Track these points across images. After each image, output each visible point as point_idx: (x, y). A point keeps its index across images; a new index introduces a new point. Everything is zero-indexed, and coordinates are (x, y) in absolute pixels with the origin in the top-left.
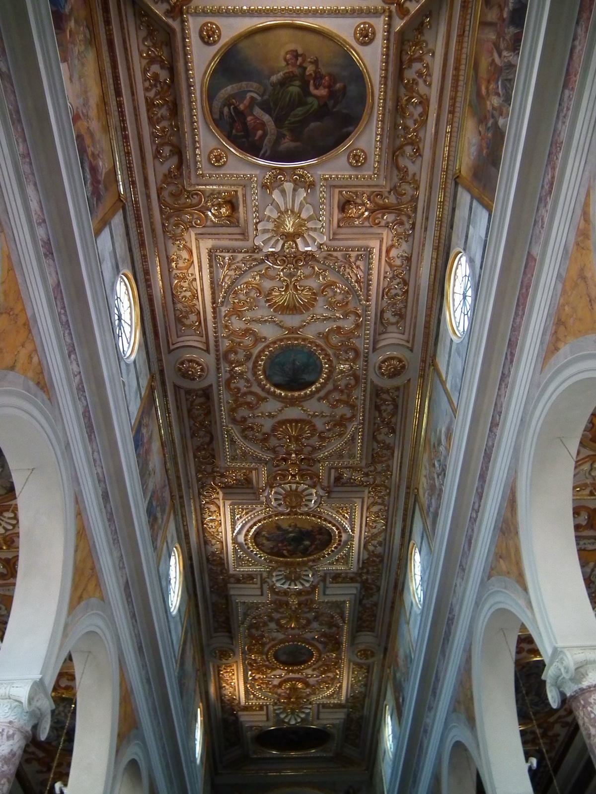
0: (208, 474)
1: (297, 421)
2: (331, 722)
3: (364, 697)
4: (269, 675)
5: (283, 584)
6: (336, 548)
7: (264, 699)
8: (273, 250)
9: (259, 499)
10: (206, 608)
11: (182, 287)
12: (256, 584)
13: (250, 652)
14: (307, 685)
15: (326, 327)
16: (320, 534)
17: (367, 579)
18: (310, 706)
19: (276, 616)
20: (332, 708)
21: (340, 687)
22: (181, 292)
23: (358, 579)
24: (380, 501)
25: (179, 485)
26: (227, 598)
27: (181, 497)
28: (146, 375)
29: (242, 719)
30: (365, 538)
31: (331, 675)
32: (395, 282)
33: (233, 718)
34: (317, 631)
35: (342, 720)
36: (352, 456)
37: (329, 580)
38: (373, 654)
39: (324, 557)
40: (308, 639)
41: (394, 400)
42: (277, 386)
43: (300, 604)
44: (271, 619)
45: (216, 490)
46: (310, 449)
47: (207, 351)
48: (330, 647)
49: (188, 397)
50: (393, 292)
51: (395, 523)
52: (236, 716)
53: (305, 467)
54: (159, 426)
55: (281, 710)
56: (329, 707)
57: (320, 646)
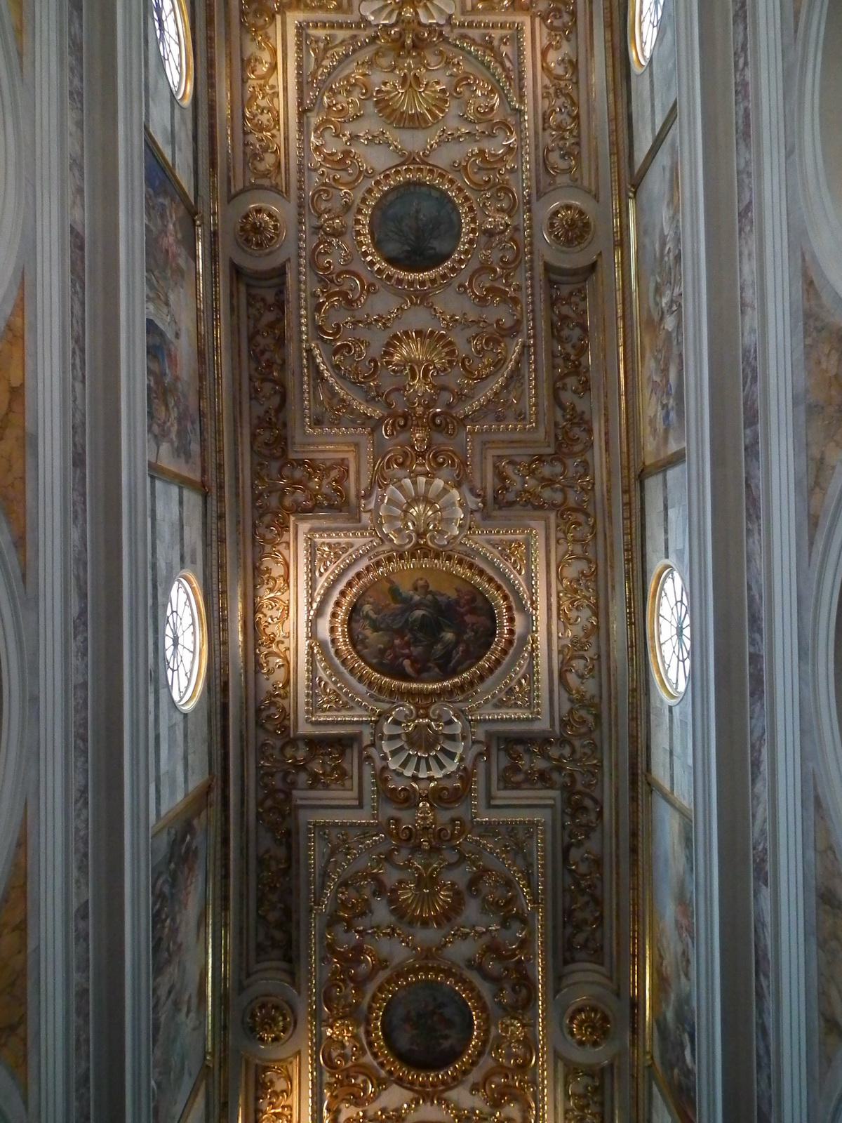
8: (387, 22)
9: (360, 521)
16: (473, 611)
30: (560, 652)
51: (613, 587)
54: (197, 273)
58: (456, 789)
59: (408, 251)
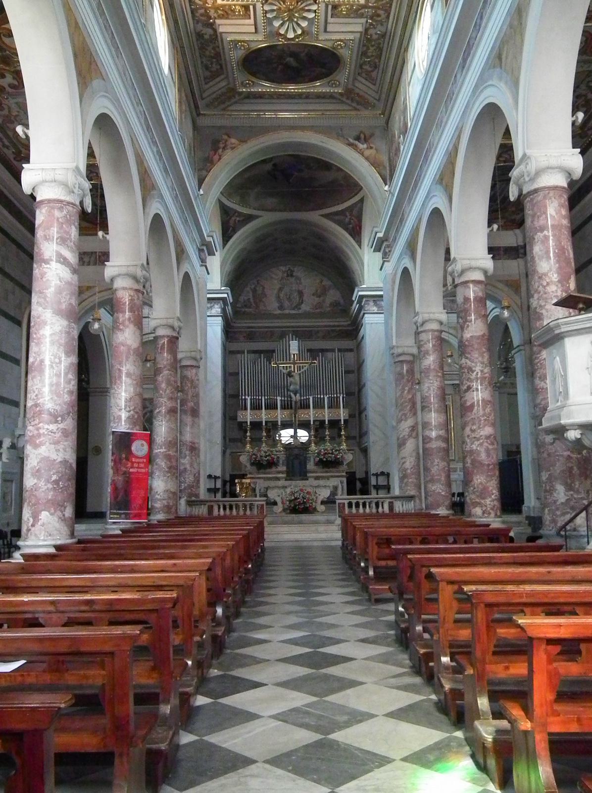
18: (314, 7)
29: (221, 29)
35: (358, 35)
52: (212, 26)
55: (274, 14)
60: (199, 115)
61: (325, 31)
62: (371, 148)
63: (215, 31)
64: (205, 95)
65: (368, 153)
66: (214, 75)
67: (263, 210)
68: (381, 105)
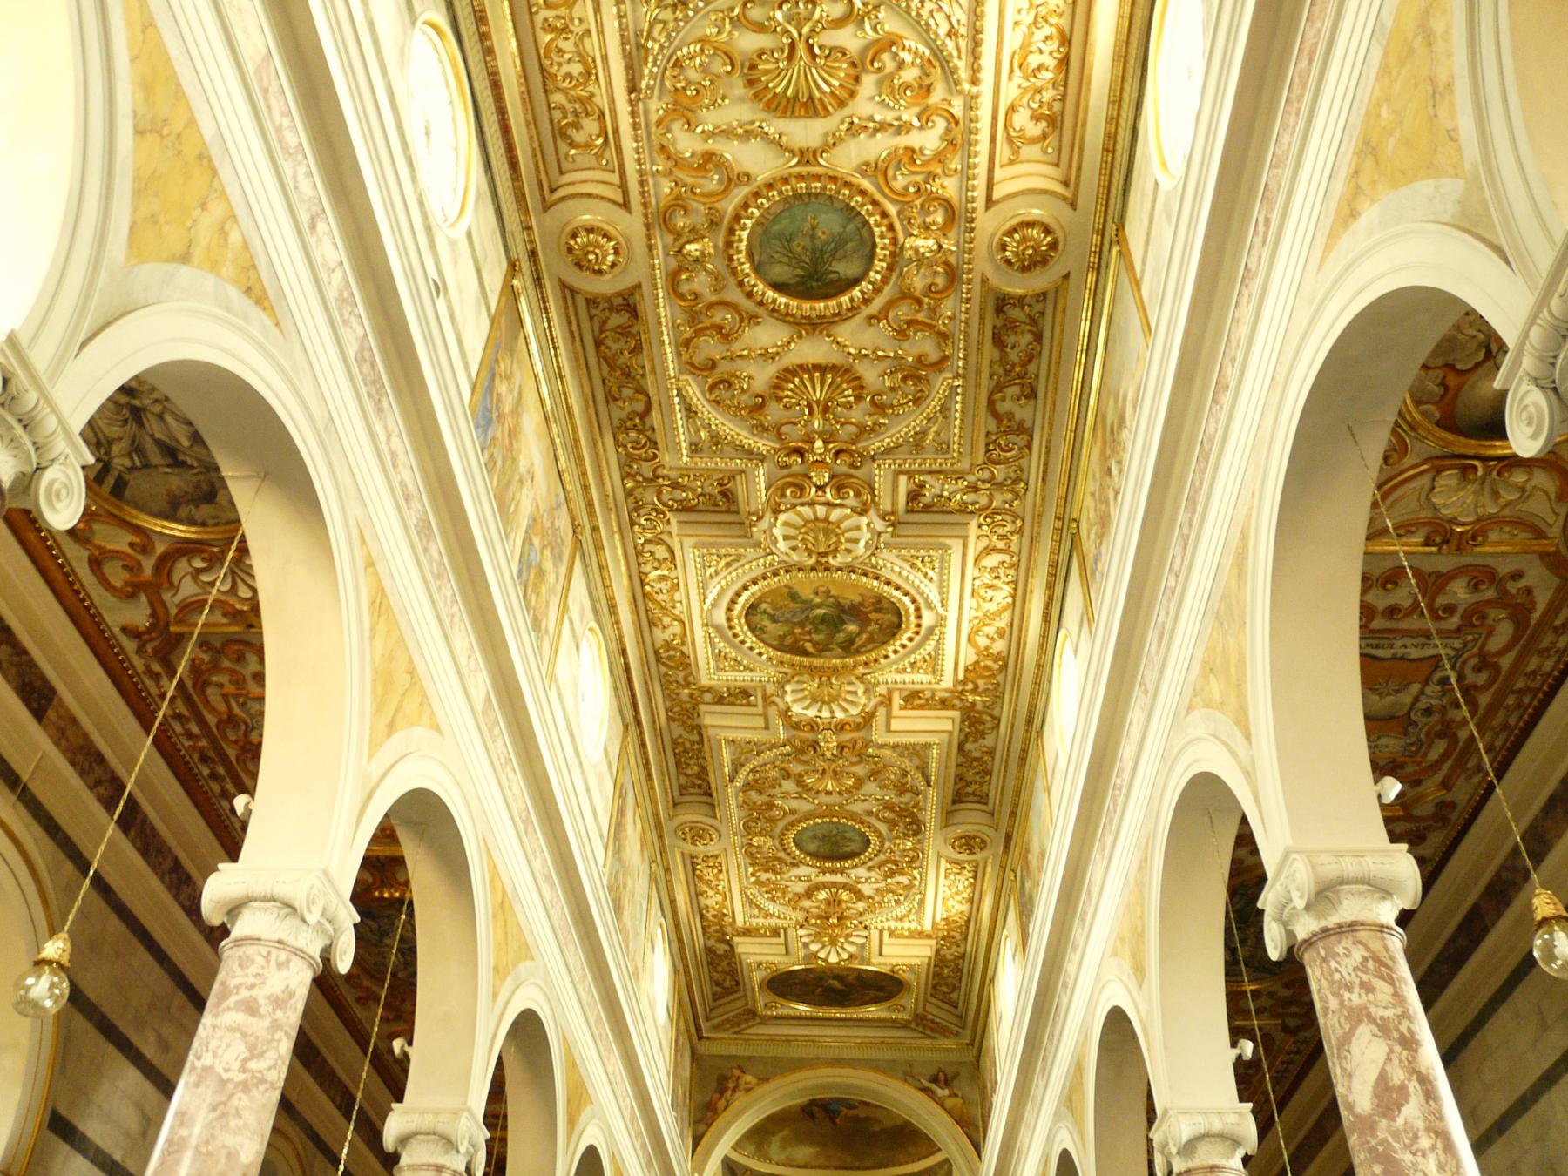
0: (645, 479)
1: (822, 369)
2: (906, 961)
3: (969, 920)
4: (785, 876)
5: (807, 708)
6: (911, 639)
7: (779, 917)
10: (662, 749)
11: (561, 51)
12: (755, 706)
13: (749, 834)
14: (860, 896)
15: (878, 147)
17: (973, 704)
18: (865, 933)
19: (796, 768)
20: (907, 937)
21: (921, 902)
22: (560, 64)
23: (956, 702)
24: (1001, 545)
25: (590, 505)
26: (699, 729)
27: (595, 529)
28: (500, 263)
29: (740, 949)
31: (904, 880)
32: (1039, 35)
33: (723, 947)
34: (876, 799)
35: (926, 960)
36: (943, 448)
37: (897, 701)
38: (983, 845)
39: (886, 657)
40: (857, 814)
41: (1033, 321)
42: (779, 287)
43: (841, 747)
44: (787, 775)
45: (665, 516)
46: (853, 429)
47: (625, 205)
48: (901, 827)
49: (594, 312)
50: (1034, 61)
52: (728, 943)
53: (845, 469)
56: (901, 936)
57: (883, 828)
58: (859, 724)
59: (803, 276)
60: (700, 1038)
61: (881, 954)
62: (956, 1095)
63: (732, 947)
64: (714, 1013)
65: (950, 1103)
66: (728, 992)
67: (791, 1166)
68: (968, 1033)
